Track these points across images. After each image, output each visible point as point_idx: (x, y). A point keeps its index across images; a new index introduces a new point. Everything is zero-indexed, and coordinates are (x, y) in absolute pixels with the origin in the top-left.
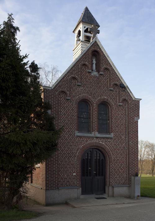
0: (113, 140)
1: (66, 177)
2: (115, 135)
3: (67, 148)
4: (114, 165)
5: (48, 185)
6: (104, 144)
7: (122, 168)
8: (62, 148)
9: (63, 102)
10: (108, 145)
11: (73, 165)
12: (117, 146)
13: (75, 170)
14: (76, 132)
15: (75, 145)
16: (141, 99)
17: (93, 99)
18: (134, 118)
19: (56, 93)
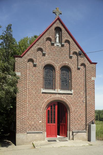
1: (33, 124)
3: (35, 102)
5: (18, 130)
6: (65, 98)
8: (30, 102)
9: (31, 67)
11: (40, 114)
13: (41, 119)
14: (42, 89)
15: (40, 100)
16: (97, 63)
17: (56, 64)
19: (25, 60)
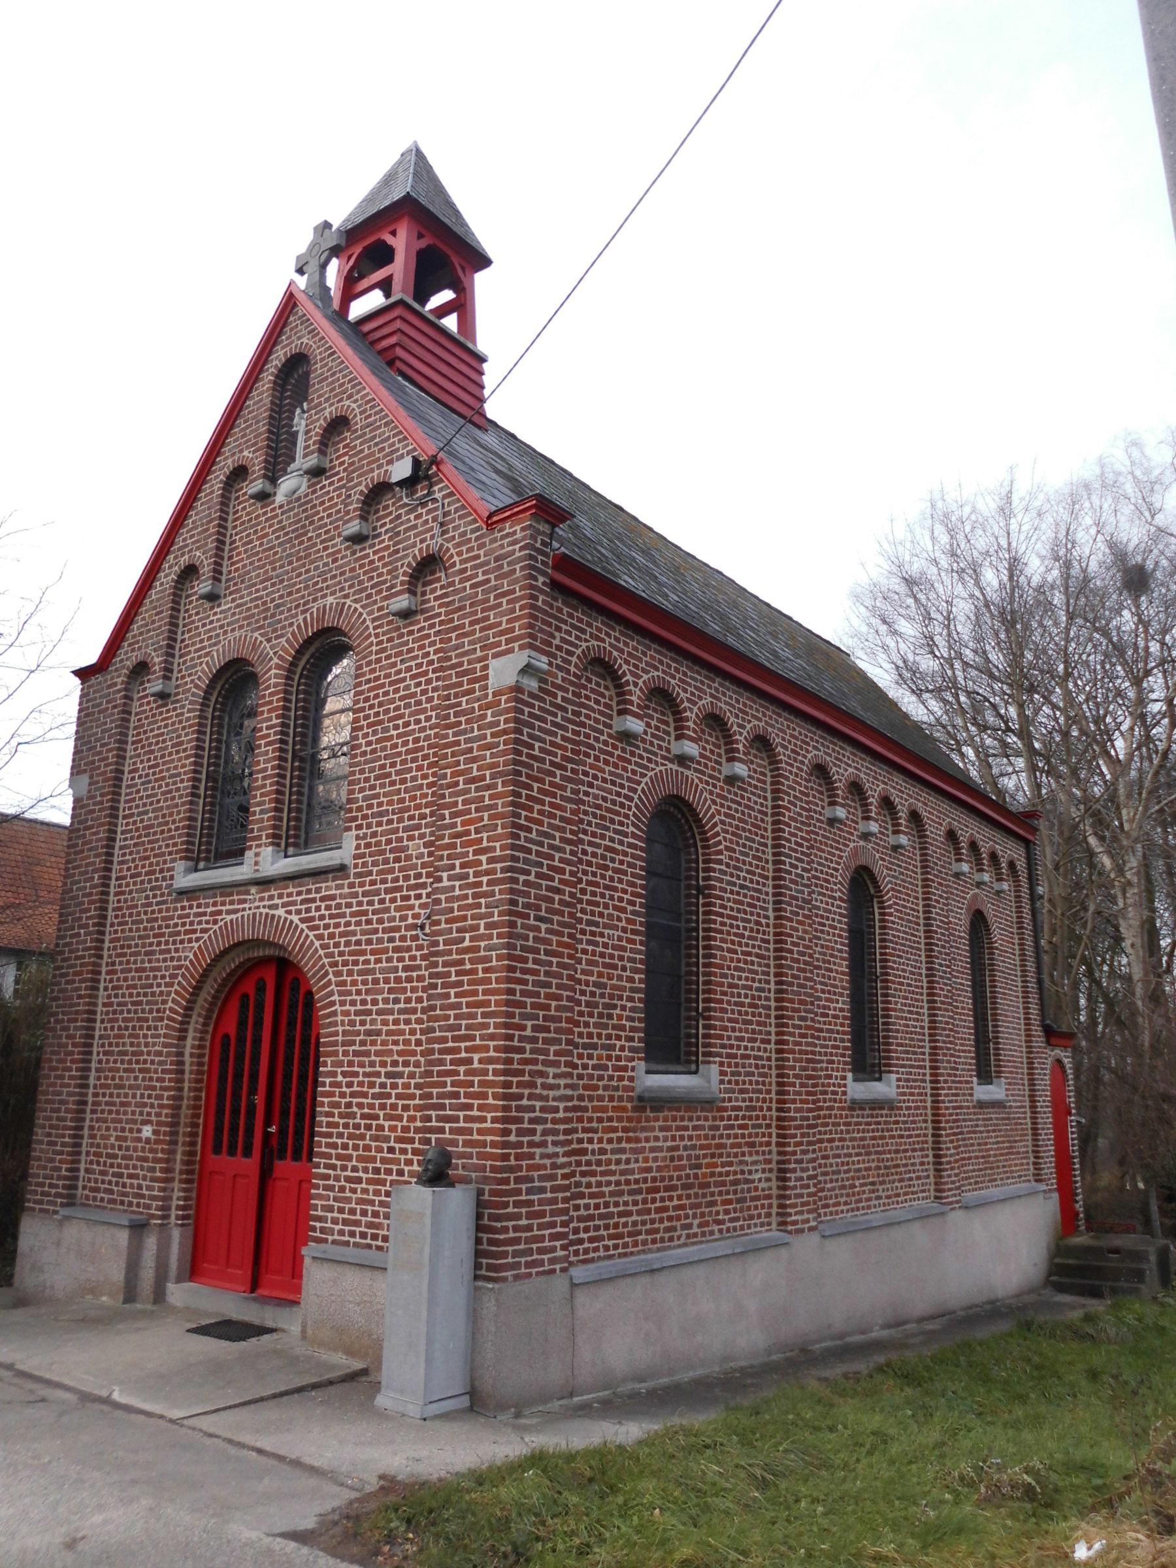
0: (352, 885)
2: (368, 845)
4: (344, 1074)
7: (394, 1107)
10: (317, 928)
12: (369, 922)
14: (180, 866)
18: (486, 667)
